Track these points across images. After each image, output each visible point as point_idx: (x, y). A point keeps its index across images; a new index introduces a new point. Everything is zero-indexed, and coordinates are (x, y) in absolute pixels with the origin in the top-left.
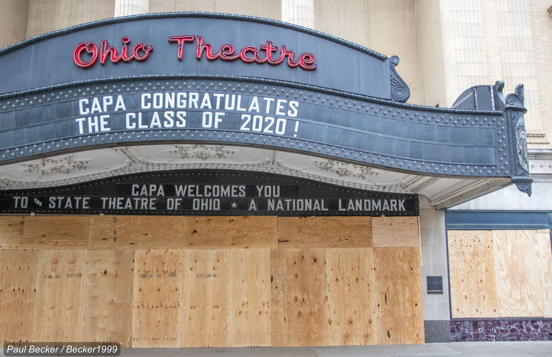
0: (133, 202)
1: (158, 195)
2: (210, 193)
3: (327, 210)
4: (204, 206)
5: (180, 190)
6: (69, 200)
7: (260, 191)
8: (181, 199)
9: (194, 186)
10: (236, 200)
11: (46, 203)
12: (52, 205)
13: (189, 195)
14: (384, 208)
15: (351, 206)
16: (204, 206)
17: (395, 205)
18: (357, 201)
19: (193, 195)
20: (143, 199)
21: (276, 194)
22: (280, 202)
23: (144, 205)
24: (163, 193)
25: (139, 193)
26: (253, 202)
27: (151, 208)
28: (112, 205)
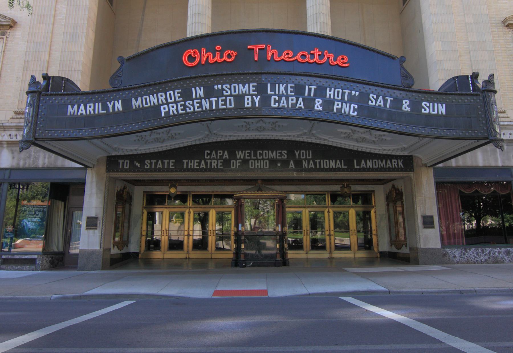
0: (206, 164)
1: (224, 158)
2: (261, 157)
3: (346, 167)
4: (258, 166)
6: (160, 162)
7: (297, 154)
8: (241, 161)
9: (249, 151)
11: (143, 164)
12: (147, 166)
14: (388, 166)
15: (363, 164)
16: (258, 166)
17: (396, 164)
18: (368, 161)
19: (249, 158)
20: (213, 161)
21: (309, 156)
22: (311, 162)
23: (214, 165)
24: (227, 157)
25: (210, 157)
26: (292, 162)
27: (219, 167)
28: (191, 165)
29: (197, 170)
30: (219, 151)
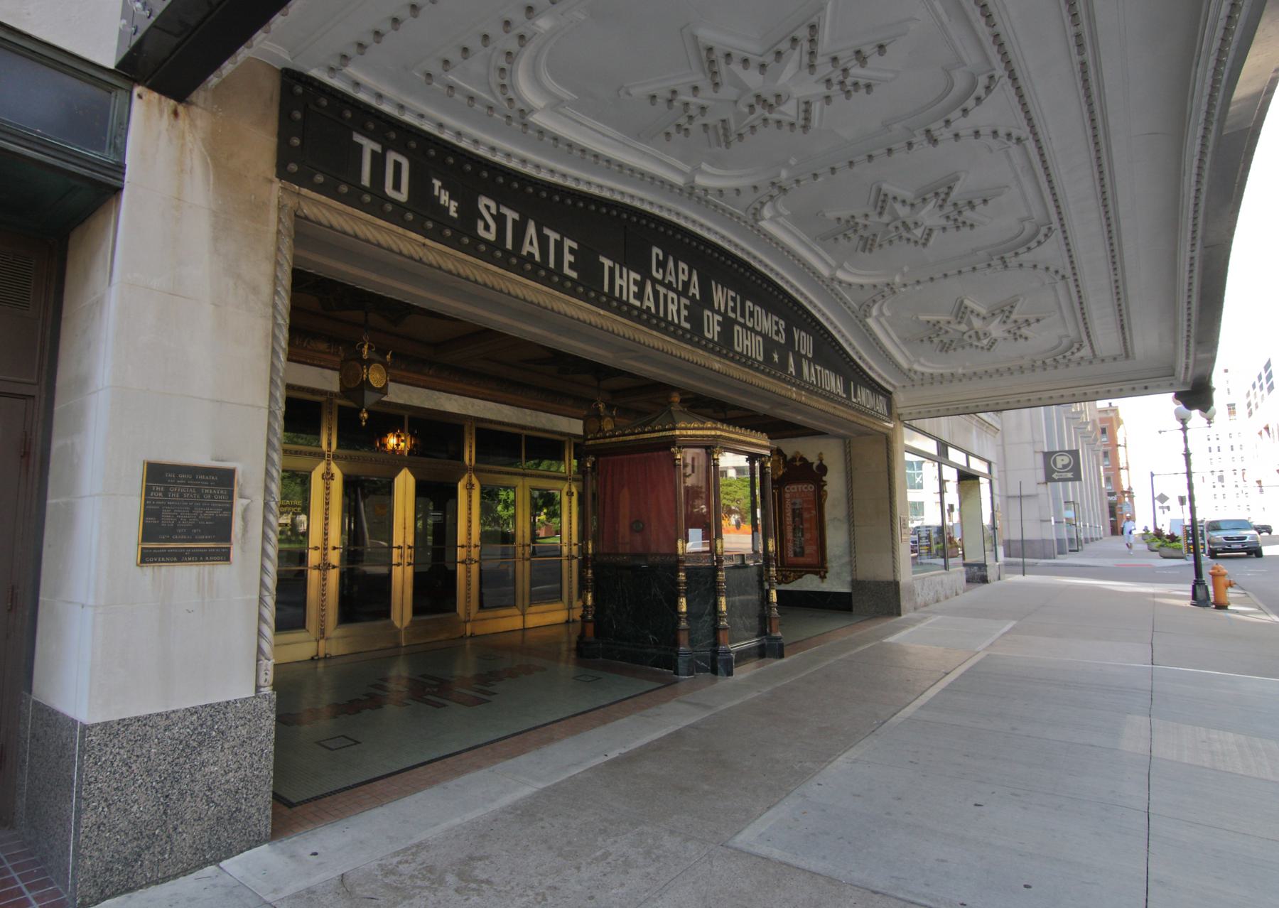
6: (531, 230)
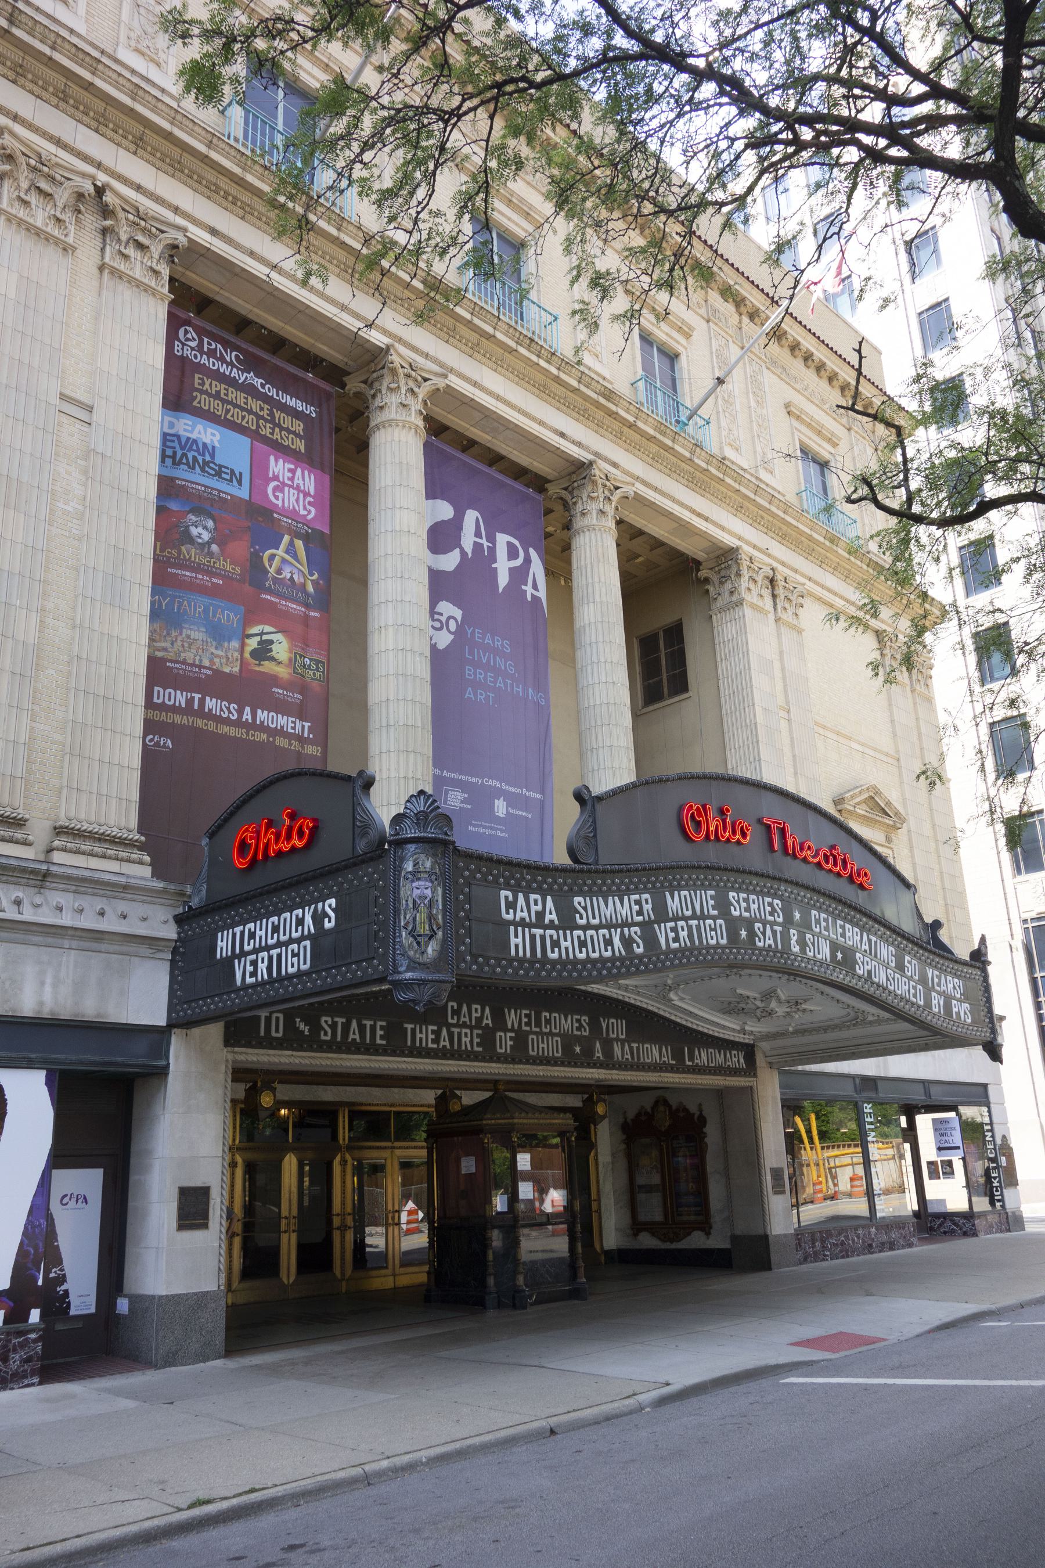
0: (451, 1035)
5: (512, 1018)
6: (354, 1024)
10: (579, 1039)
11: (316, 1028)
13: (524, 1028)
20: (464, 1031)
24: (490, 1022)
26: (598, 1045)
27: (476, 1049)
29: (428, 1054)
30: (474, 1006)
